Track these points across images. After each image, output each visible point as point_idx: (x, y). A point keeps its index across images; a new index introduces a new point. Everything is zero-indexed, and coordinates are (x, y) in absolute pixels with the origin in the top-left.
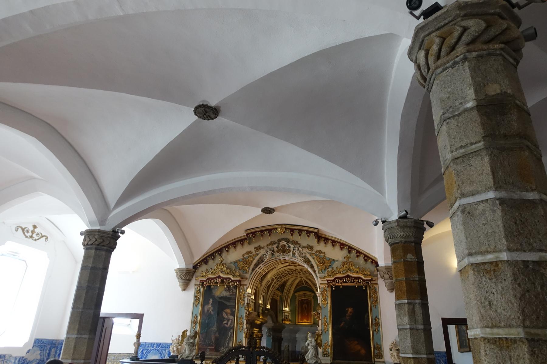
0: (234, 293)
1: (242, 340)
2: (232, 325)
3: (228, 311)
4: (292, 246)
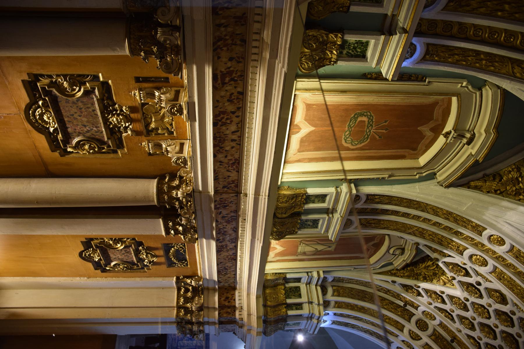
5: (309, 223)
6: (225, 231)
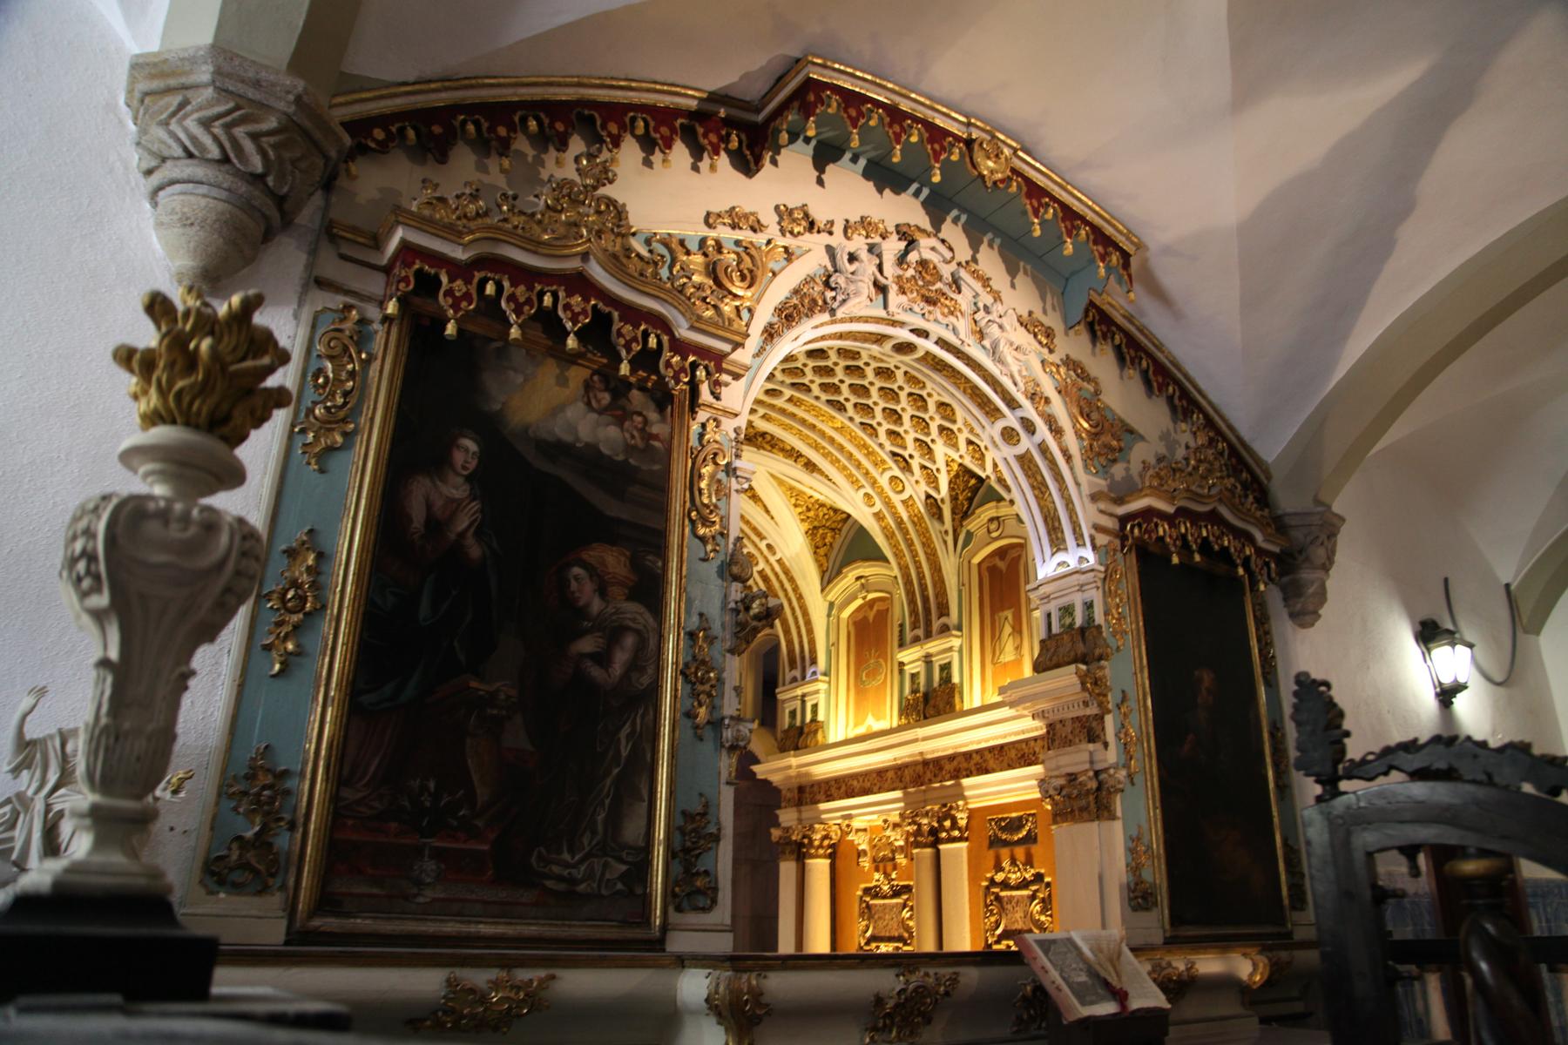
0: (657, 444)
2: (645, 680)
3: (614, 561)
5: (944, 675)
6: (955, 770)
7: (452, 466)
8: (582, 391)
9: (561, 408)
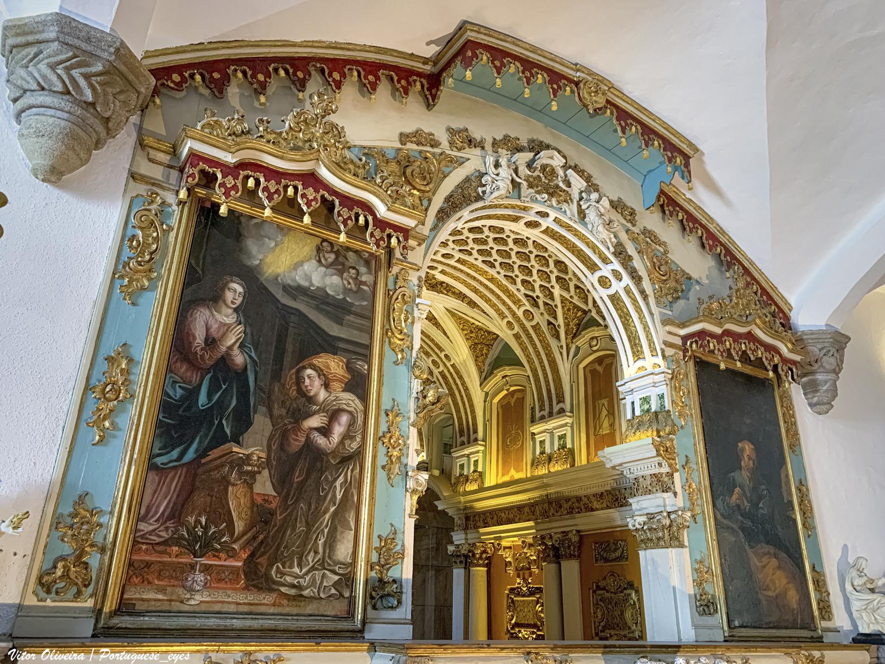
0: (365, 288)
1: (398, 525)
2: (355, 445)
3: (335, 365)
4: (578, 183)
5: (562, 442)
6: (570, 508)
7: (225, 302)
8: (315, 253)
9: (300, 264)
